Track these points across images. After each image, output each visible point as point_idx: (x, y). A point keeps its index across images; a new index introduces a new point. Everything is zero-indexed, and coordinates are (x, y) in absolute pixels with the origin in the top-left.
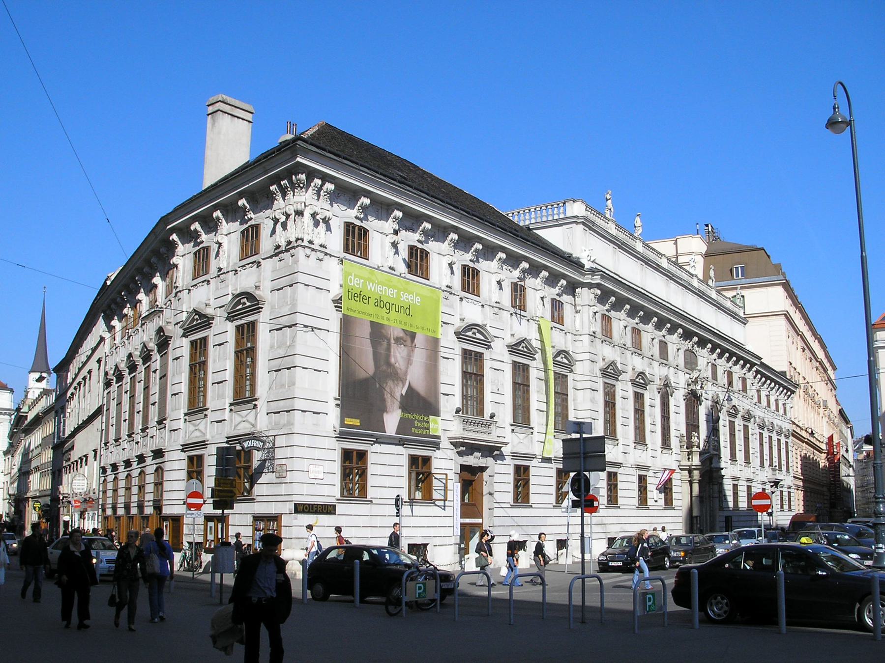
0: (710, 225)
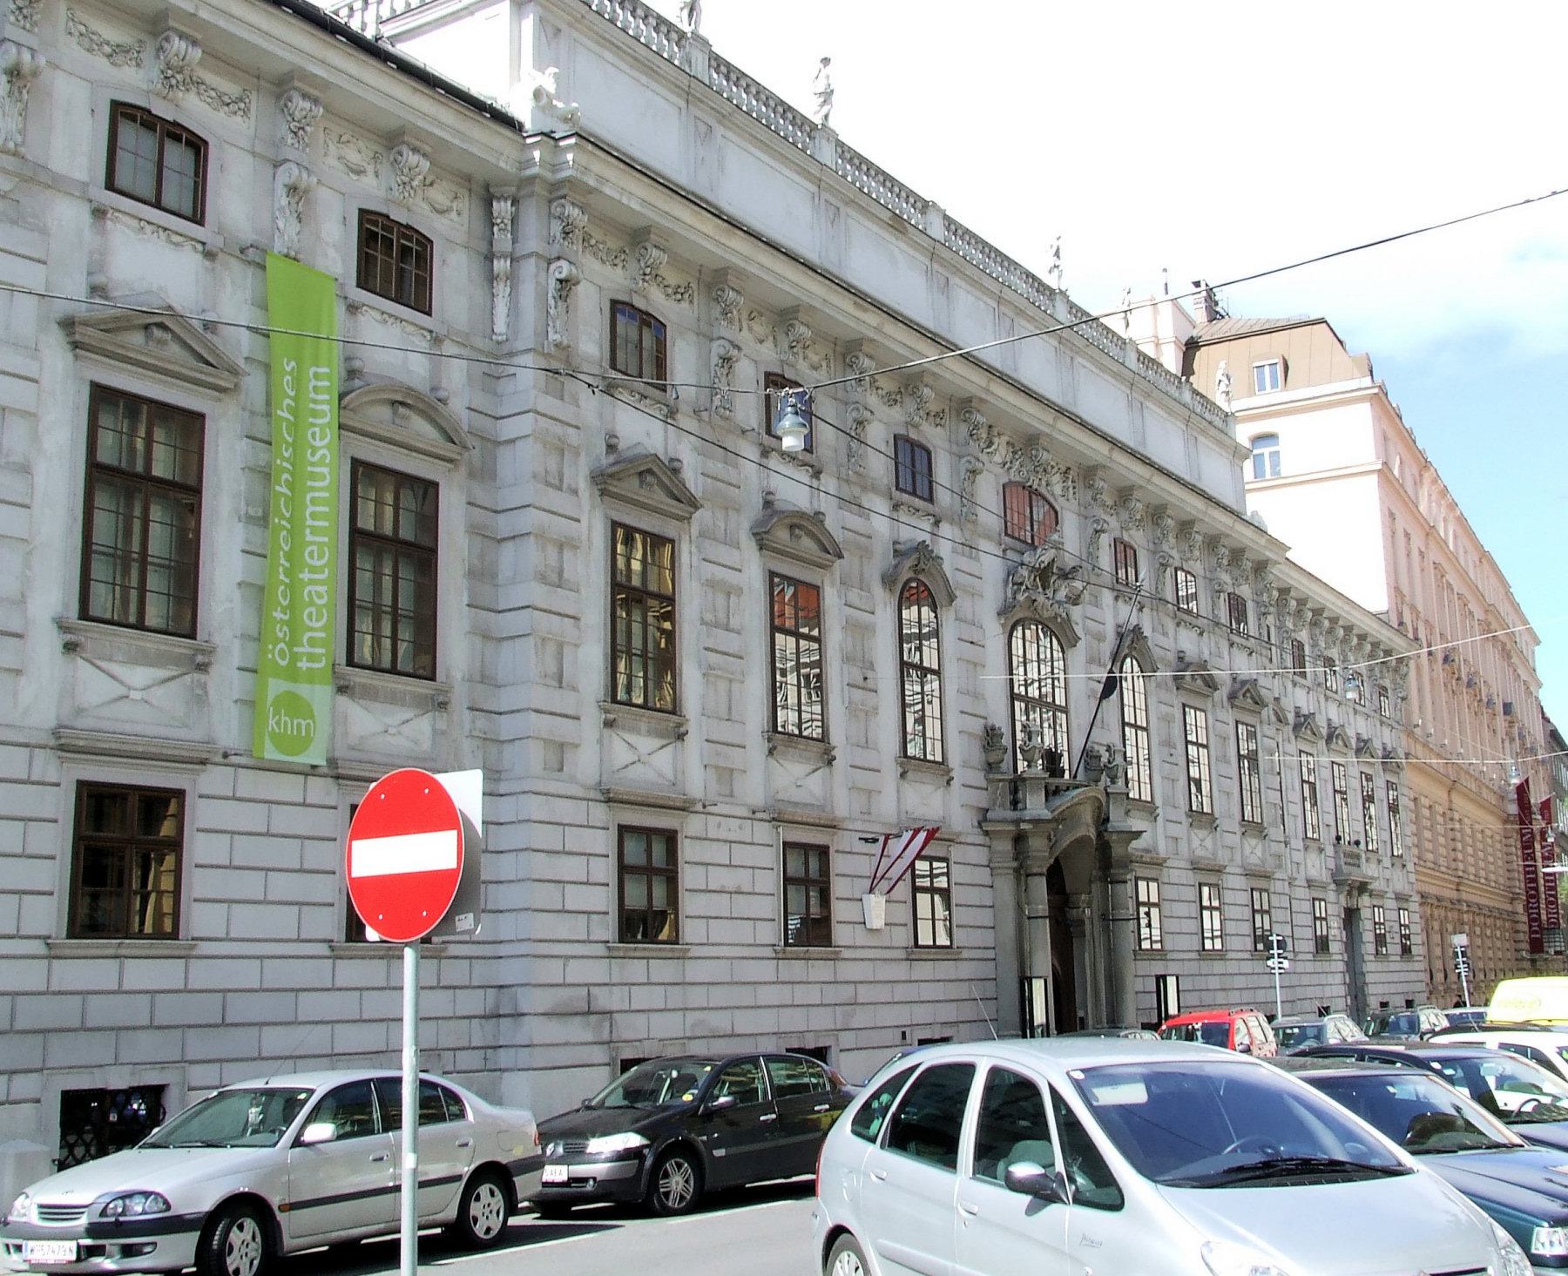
0: (1203, 284)
